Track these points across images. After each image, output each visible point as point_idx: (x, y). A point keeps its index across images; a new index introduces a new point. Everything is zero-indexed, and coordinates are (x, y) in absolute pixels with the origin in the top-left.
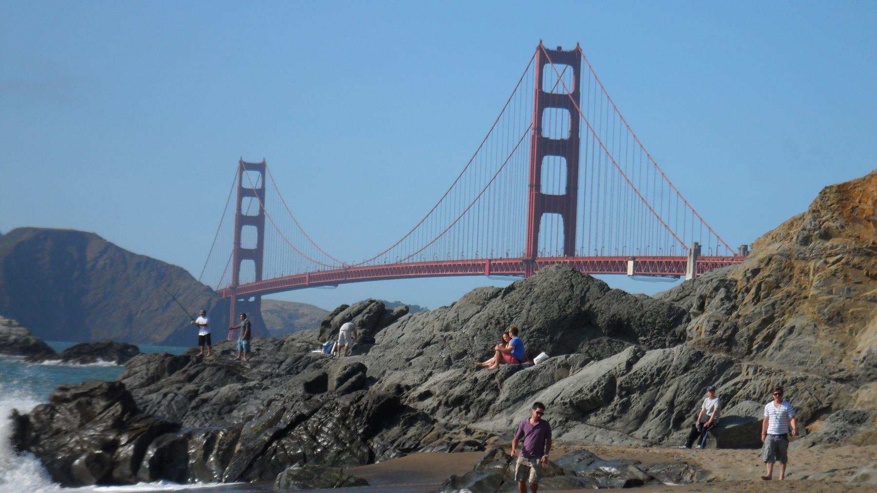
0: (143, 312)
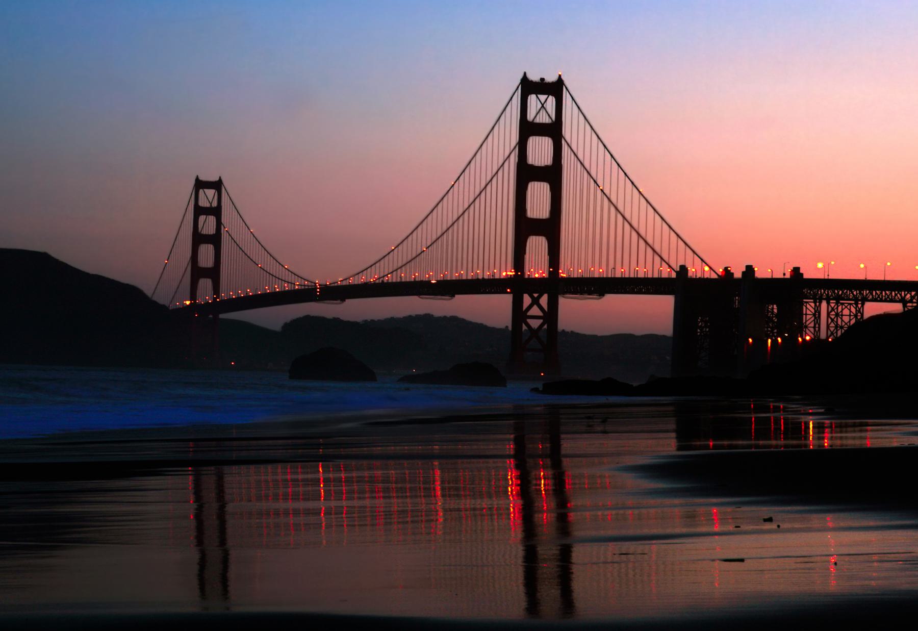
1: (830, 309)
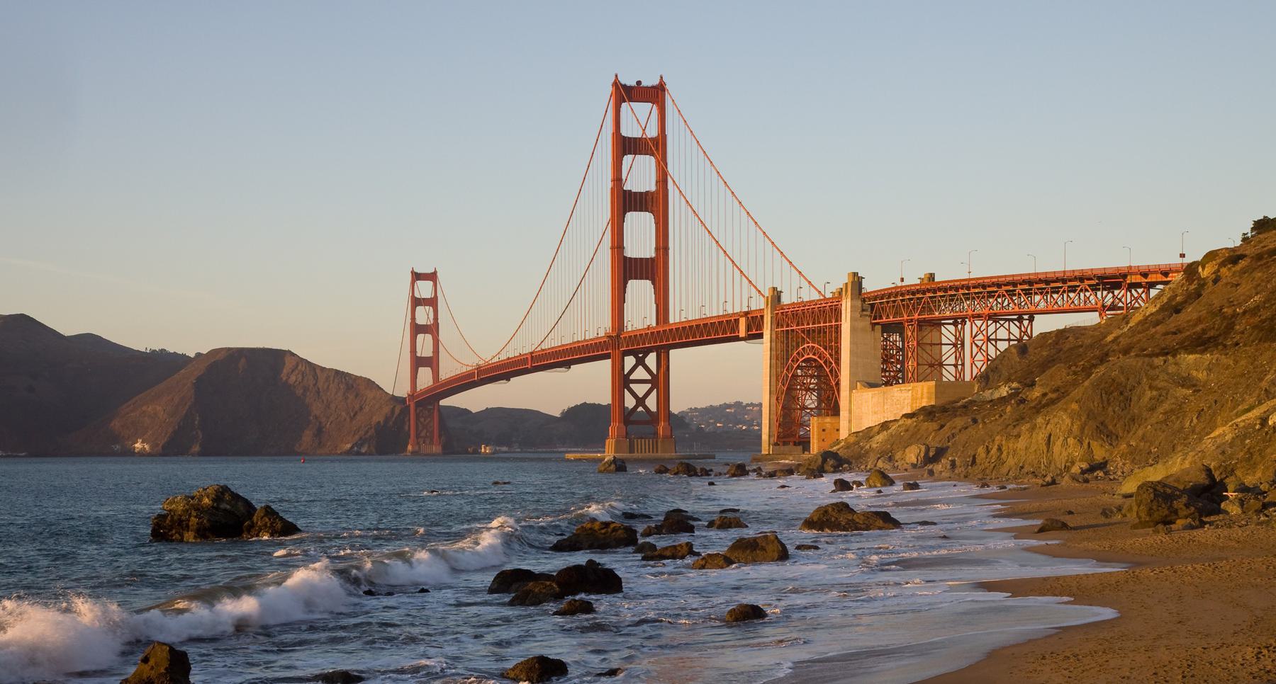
0: (331, 422)
1: (975, 330)
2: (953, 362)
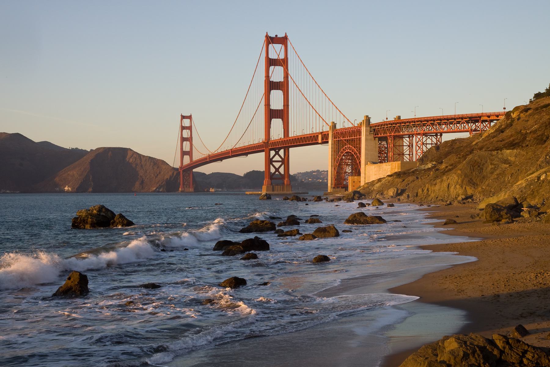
2: (408, 153)
